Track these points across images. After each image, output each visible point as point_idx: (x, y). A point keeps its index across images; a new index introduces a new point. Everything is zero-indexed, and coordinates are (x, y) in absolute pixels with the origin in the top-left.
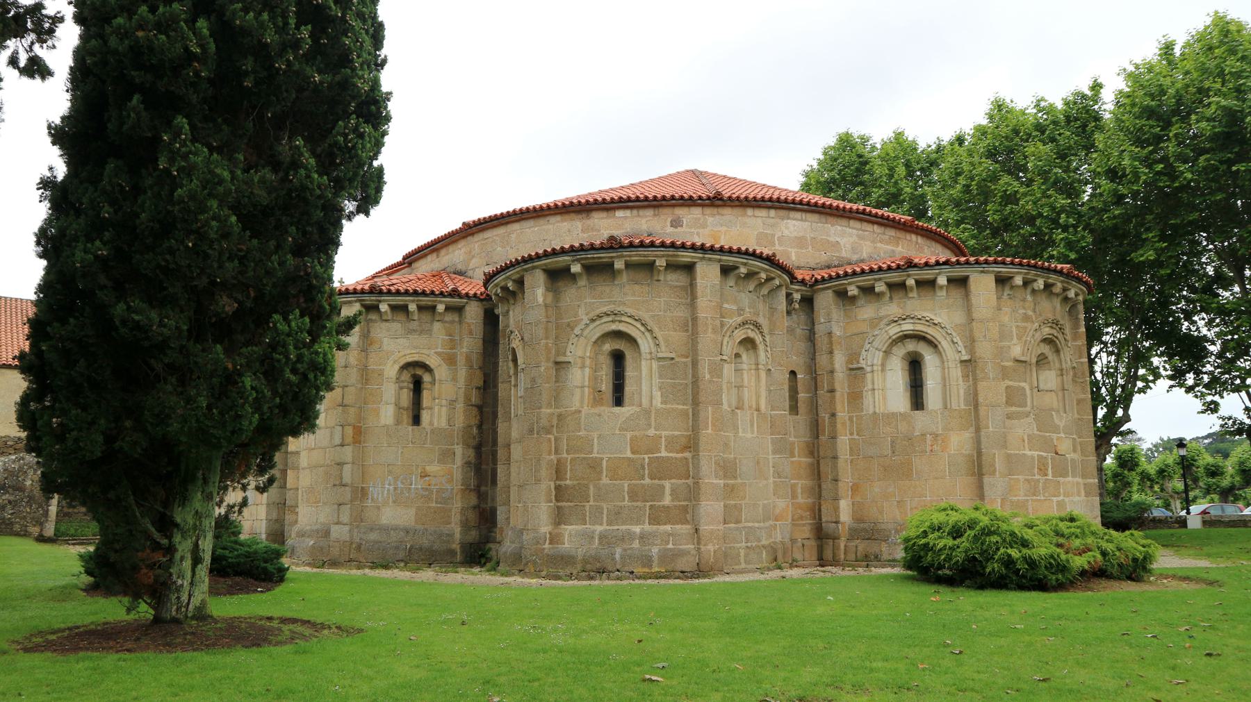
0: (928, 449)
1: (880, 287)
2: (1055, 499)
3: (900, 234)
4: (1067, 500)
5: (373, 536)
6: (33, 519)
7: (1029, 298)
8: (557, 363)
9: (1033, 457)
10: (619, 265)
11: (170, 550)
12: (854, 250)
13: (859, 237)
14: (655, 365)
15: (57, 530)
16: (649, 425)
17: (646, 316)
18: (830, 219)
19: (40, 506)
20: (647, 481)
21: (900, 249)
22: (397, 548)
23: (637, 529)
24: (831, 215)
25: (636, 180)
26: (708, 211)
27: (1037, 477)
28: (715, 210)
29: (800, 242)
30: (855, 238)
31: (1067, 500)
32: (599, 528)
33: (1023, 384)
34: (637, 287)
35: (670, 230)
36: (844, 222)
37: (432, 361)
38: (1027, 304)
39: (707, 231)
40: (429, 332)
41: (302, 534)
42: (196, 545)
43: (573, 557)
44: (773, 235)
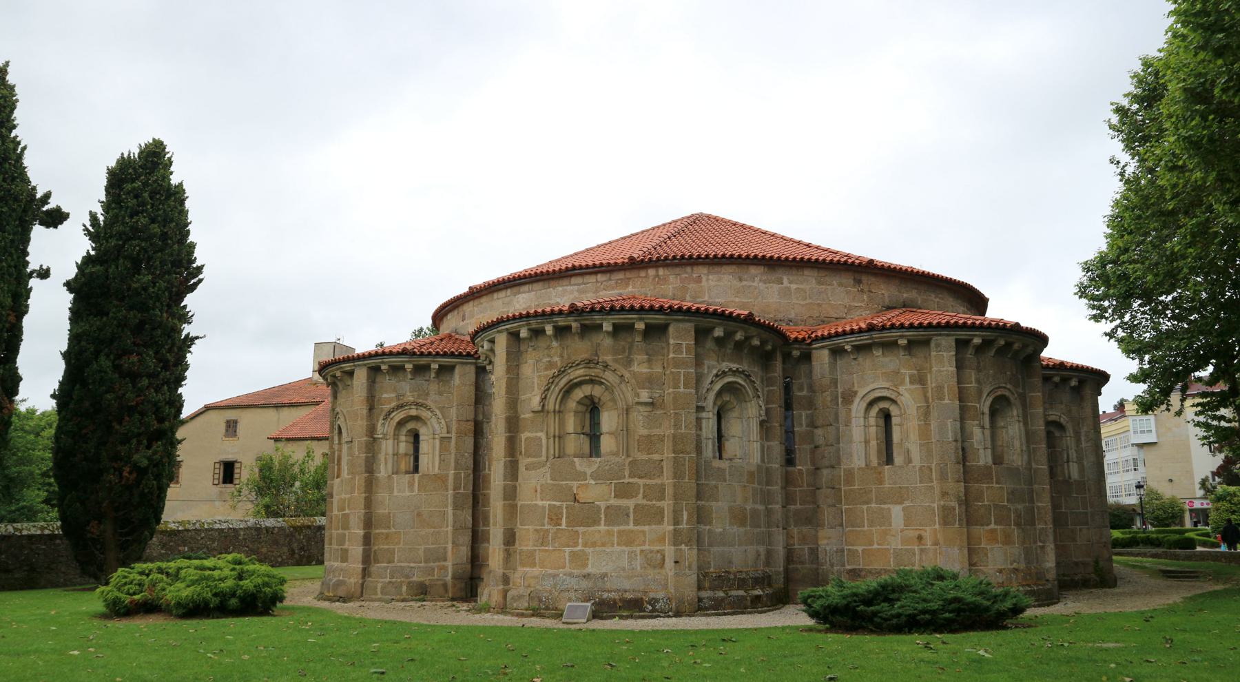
3: (628, 274)
4: (587, 550)
7: (555, 344)
9: (544, 507)
13: (580, 292)
18: (552, 283)
21: (630, 289)
24: (553, 279)
28: (476, 302)
30: (576, 294)
31: (587, 550)
33: (539, 434)
36: (565, 282)
38: (553, 351)
41: (973, 554)
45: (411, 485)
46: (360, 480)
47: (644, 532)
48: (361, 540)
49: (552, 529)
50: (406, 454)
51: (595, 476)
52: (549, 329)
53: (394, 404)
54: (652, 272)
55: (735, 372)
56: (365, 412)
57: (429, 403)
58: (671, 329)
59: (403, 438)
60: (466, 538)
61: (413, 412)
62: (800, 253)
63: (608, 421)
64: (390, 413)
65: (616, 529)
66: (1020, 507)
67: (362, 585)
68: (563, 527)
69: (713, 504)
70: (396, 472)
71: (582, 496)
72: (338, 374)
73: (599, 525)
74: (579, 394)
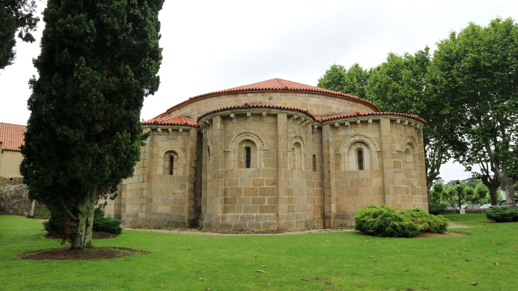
0: (365, 184)
1: (347, 123)
3: (354, 103)
5: (155, 217)
6: (25, 209)
7: (402, 128)
8: (225, 151)
9: (403, 188)
10: (249, 114)
11: (78, 221)
12: (337, 109)
13: (340, 105)
14: (262, 152)
15: (35, 213)
16: (260, 175)
17: (259, 134)
18: (328, 97)
19: (28, 204)
20: (259, 196)
21: (355, 109)
22: (164, 221)
23: (255, 215)
24: (329, 96)
26: (283, 94)
28: (285, 94)
29: (317, 106)
30: (338, 105)
32: (240, 214)
33: (400, 160)
34: (255, 123)
35: (268, 101)
36: (334, 99)
37: (177, 150)
39: (282, 102)
40: (177, 139)
41: (127, 216)
42: (87, 220)
43: (230, 225)
44: (307, 104)
49: (407, 196)
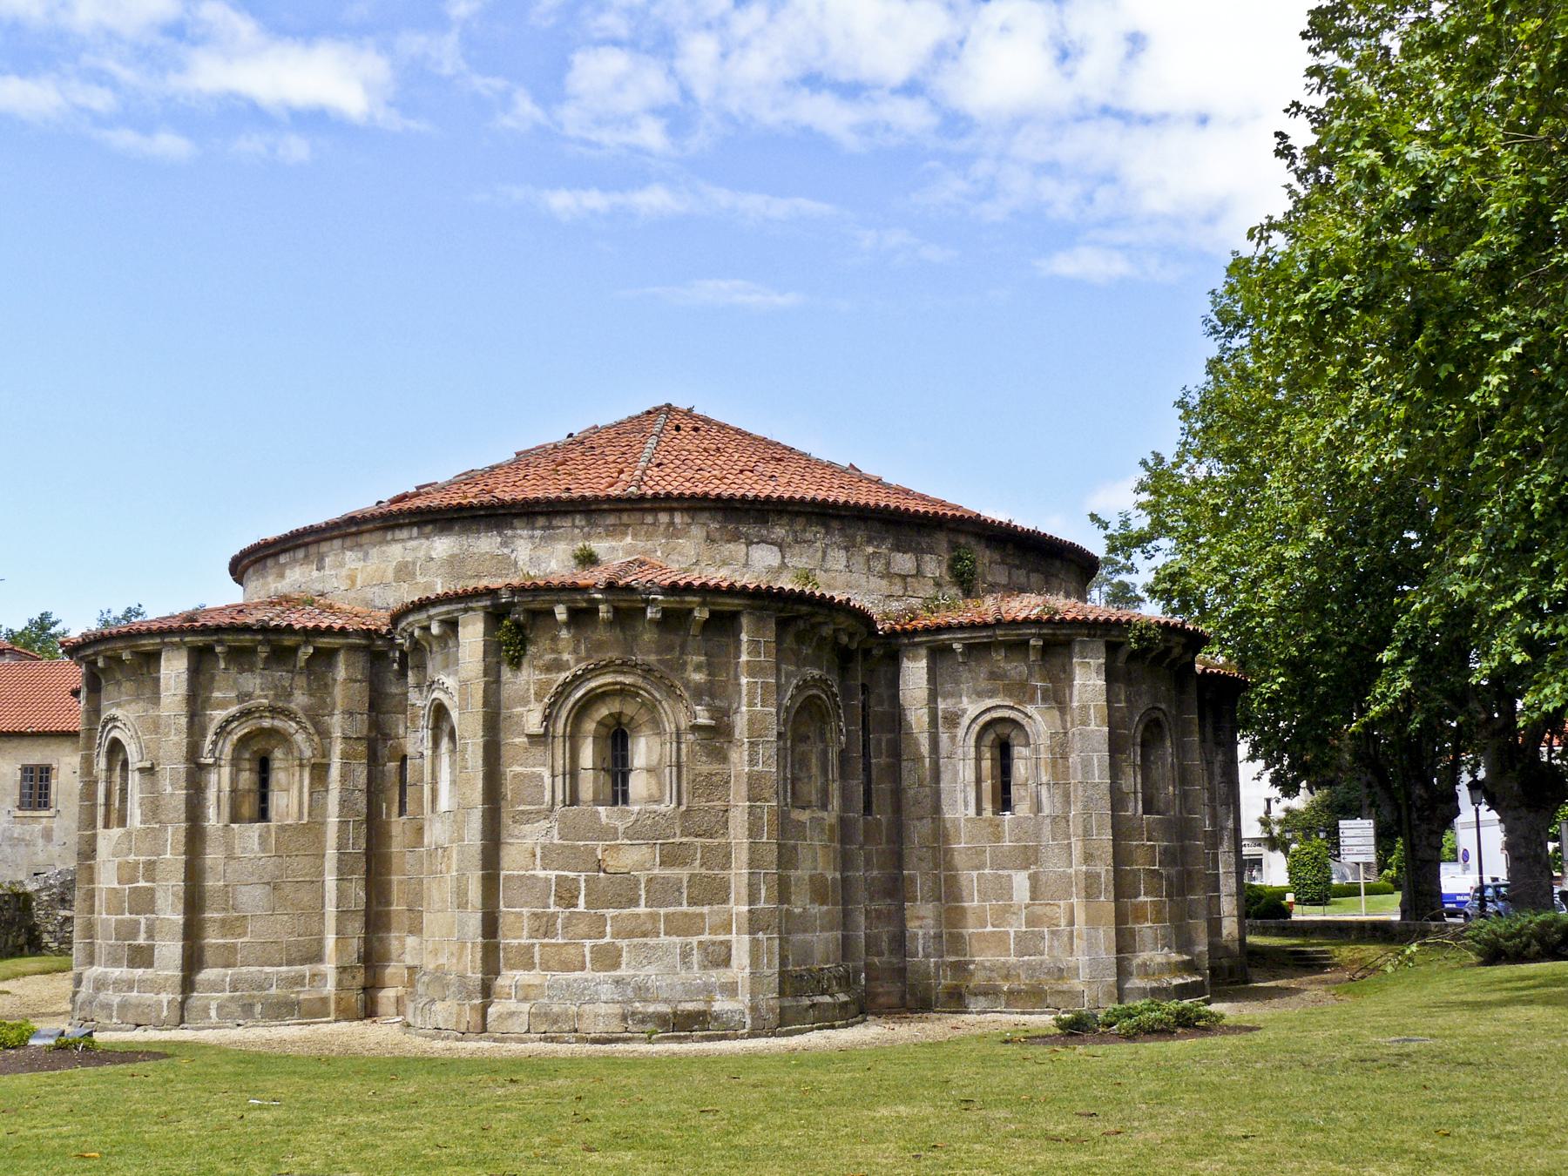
2: (588, 943)
7: (564, 634)
9: (547, 880)
20: (127, 916)
25: (443, 474)
27: (552, 910)
31: (623, 943)
39: (344, 572)
45: (263, 840)
46: (175, 834)
47: (702, 915)
48: (179, 930)
49: (562, 913)
50: (250, 791)
51: (634, 833)
52: (561, 613)
53: (234, 709)
54: (664, 518)
55: (816, 682)
56: (184, 721)
57: (293, 706)
58: (745, 621)
59: (247, 765)
60: (356, 927)
61: (267, 723)
62: (863, 497)
63: (643, 751)
64: (228, 722)
65: (662, 911)
66: (1173, 871)
67: (183, 1003)
68: (581, 907)
69: (792, 872)
70: (235, 818)
71: (612, 863)
72: (126, 656)
73: (638, 905)
74: (603, 711)
